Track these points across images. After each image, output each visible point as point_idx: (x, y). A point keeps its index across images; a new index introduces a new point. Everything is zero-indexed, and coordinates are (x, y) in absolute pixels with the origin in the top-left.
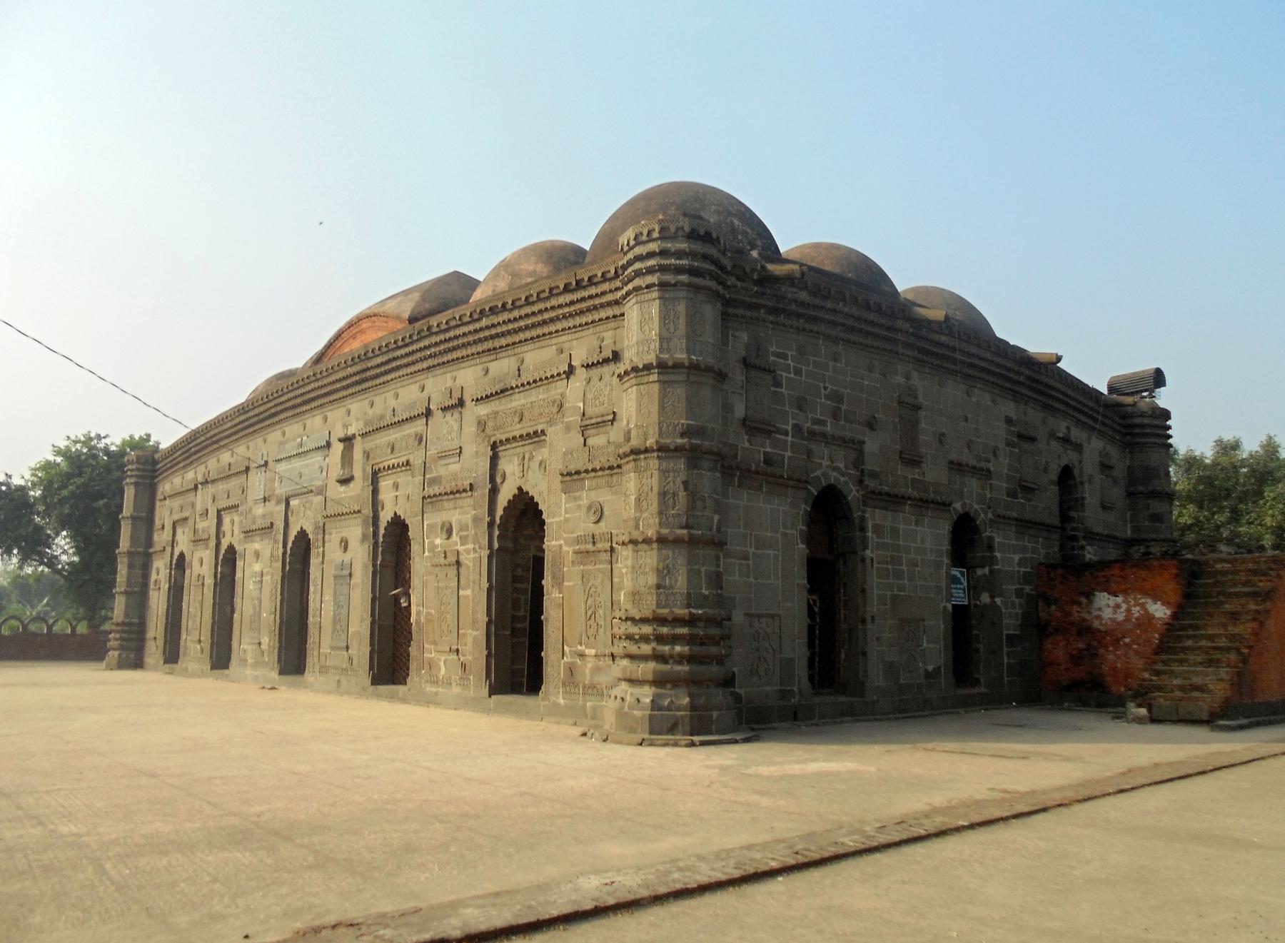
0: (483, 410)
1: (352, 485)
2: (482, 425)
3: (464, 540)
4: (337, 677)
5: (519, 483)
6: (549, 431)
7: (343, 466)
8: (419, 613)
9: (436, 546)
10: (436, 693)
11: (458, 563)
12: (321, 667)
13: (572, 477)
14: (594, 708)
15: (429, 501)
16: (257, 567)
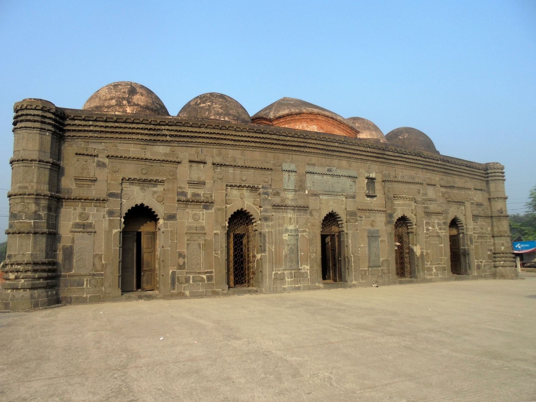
0: (443, 190)
1: (375, 199)
2: (443, 194)
3: (440, 229)
4: (375, 279)
5: (455, 214)
7: (367, 189)
8: (422, 253)
9: (430, 230)
10: (432, 278)
11: (439, 236)
12: (362, 275)
13: (475, 217)
14: (485, 275)
15: (428, 214)
16: (291, 227)
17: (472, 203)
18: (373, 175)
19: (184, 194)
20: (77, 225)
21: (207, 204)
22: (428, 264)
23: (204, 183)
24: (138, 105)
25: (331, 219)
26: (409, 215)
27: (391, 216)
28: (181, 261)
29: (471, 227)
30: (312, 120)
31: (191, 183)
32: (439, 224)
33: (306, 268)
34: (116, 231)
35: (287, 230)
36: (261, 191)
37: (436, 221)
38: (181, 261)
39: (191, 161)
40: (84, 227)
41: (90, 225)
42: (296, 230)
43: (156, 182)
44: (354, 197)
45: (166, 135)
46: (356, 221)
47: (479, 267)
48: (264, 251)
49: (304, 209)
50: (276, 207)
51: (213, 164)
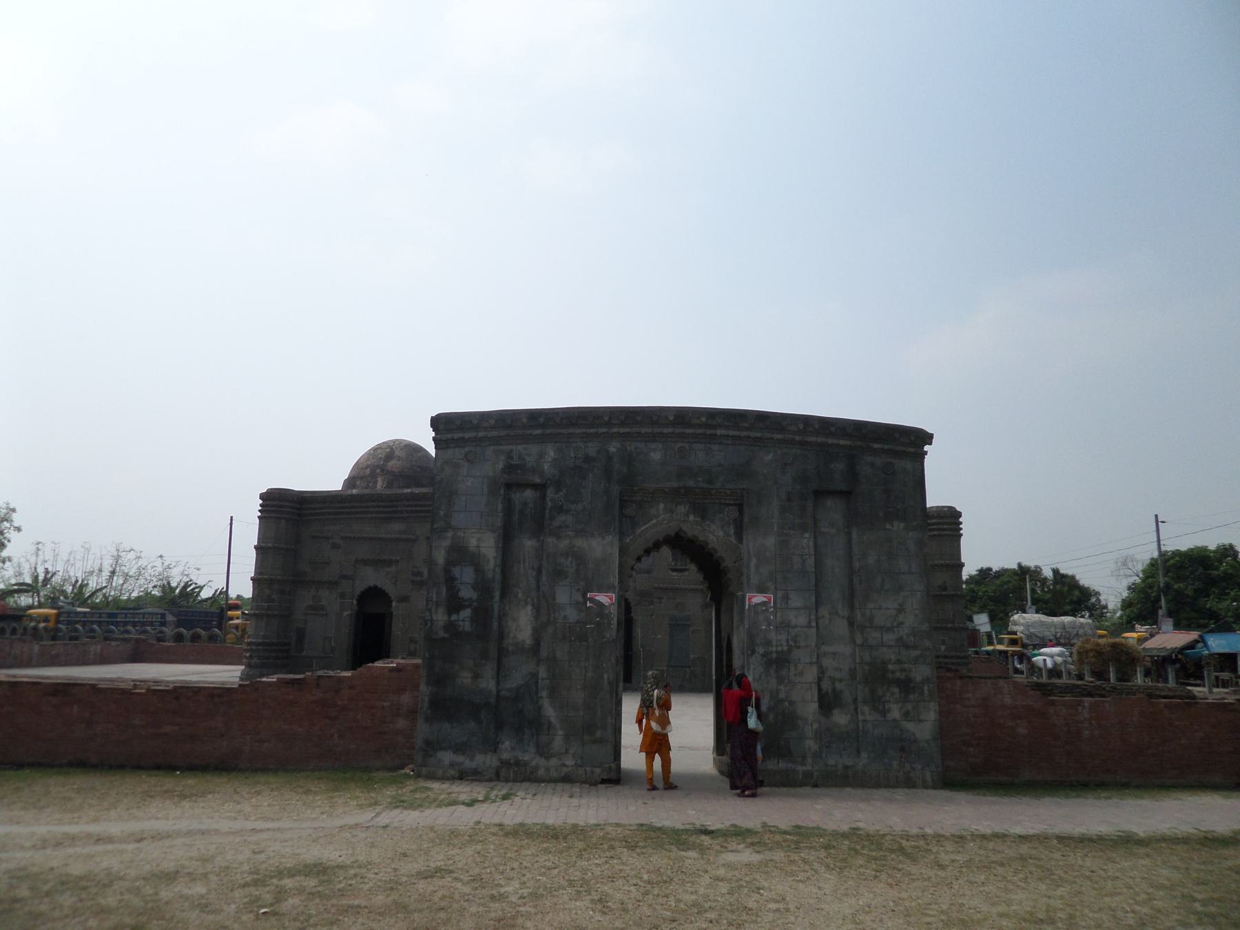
19: (419, 574)
28: (412, 647)
43: (390, 563)
45: (401, 512)
46: (652, 603)
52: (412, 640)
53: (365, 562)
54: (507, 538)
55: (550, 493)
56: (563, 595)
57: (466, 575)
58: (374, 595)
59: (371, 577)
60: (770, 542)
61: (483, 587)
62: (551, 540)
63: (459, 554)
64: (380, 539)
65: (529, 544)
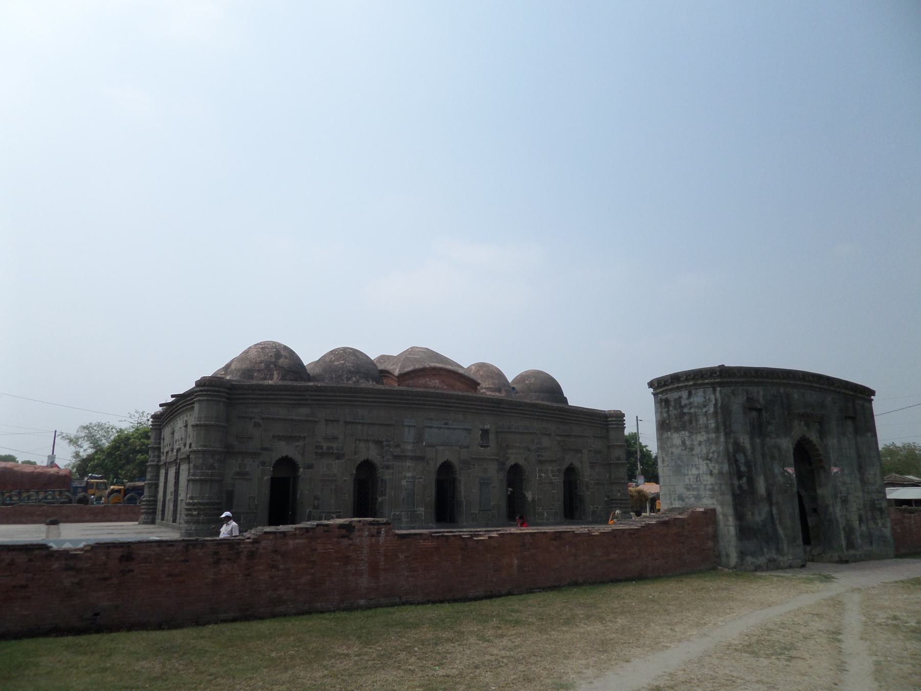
0: (559, 438)
6: (584, 451)
15: (541, 462)
17: (590, 451)
18: (487, 427)
19: (321, 447)
20: (238, 473)
21: (339, 457)
22: (539, 509)
23: (337, 438)
24: (283, 368)
25: (446, 469)
26: (521, 462)
27: (503, 464)
28: (316, 503)
29: (587, 475)
30: (434, 375)
31: (326, 439)
32: (552, 471)
33: (421, 510)
34: (267, 478)
35: (405, 477)
36: (385, 443)
37: (550, 468)
38: (316, 503)
39: (327, 420)
40: (242, 474)
41: (247, 473)
42: (414, 477)
43: (297, 439)
44: (468, 447)
47: (594, 513)
48: (385, 495)
49: (420, 459)
50: (397, 458)
51: (346, 423)
52: (316, 498)
53: (280, 438)
54: (752, 438)
55: (764, 415)
56: (777, 470)
57: (741, 458)
58: (287, 463)
59: (284, 450)
60: (835, 441)
61: (748, 464)
62: (768, 439)
63: (738, 448)
64: (292, 420)
65: (758, 441)
